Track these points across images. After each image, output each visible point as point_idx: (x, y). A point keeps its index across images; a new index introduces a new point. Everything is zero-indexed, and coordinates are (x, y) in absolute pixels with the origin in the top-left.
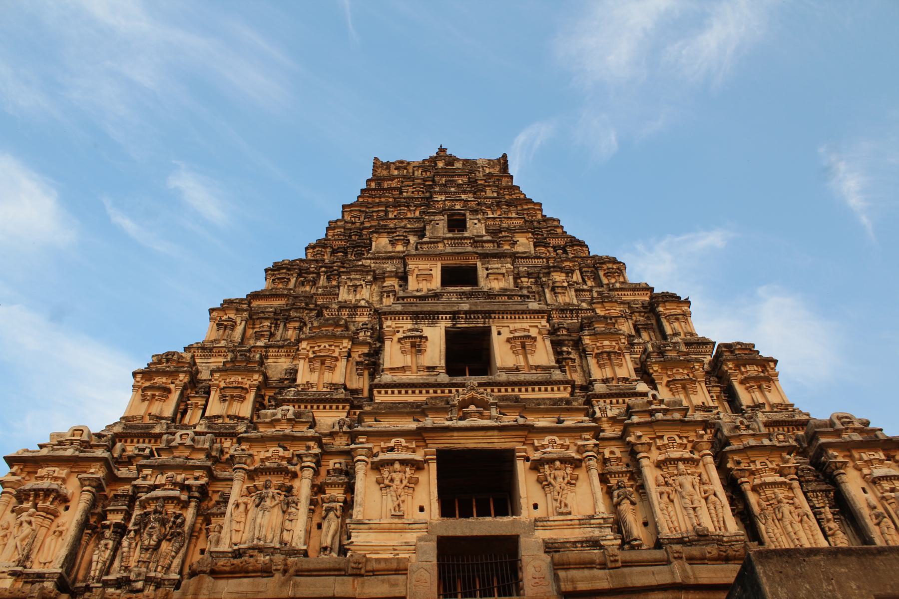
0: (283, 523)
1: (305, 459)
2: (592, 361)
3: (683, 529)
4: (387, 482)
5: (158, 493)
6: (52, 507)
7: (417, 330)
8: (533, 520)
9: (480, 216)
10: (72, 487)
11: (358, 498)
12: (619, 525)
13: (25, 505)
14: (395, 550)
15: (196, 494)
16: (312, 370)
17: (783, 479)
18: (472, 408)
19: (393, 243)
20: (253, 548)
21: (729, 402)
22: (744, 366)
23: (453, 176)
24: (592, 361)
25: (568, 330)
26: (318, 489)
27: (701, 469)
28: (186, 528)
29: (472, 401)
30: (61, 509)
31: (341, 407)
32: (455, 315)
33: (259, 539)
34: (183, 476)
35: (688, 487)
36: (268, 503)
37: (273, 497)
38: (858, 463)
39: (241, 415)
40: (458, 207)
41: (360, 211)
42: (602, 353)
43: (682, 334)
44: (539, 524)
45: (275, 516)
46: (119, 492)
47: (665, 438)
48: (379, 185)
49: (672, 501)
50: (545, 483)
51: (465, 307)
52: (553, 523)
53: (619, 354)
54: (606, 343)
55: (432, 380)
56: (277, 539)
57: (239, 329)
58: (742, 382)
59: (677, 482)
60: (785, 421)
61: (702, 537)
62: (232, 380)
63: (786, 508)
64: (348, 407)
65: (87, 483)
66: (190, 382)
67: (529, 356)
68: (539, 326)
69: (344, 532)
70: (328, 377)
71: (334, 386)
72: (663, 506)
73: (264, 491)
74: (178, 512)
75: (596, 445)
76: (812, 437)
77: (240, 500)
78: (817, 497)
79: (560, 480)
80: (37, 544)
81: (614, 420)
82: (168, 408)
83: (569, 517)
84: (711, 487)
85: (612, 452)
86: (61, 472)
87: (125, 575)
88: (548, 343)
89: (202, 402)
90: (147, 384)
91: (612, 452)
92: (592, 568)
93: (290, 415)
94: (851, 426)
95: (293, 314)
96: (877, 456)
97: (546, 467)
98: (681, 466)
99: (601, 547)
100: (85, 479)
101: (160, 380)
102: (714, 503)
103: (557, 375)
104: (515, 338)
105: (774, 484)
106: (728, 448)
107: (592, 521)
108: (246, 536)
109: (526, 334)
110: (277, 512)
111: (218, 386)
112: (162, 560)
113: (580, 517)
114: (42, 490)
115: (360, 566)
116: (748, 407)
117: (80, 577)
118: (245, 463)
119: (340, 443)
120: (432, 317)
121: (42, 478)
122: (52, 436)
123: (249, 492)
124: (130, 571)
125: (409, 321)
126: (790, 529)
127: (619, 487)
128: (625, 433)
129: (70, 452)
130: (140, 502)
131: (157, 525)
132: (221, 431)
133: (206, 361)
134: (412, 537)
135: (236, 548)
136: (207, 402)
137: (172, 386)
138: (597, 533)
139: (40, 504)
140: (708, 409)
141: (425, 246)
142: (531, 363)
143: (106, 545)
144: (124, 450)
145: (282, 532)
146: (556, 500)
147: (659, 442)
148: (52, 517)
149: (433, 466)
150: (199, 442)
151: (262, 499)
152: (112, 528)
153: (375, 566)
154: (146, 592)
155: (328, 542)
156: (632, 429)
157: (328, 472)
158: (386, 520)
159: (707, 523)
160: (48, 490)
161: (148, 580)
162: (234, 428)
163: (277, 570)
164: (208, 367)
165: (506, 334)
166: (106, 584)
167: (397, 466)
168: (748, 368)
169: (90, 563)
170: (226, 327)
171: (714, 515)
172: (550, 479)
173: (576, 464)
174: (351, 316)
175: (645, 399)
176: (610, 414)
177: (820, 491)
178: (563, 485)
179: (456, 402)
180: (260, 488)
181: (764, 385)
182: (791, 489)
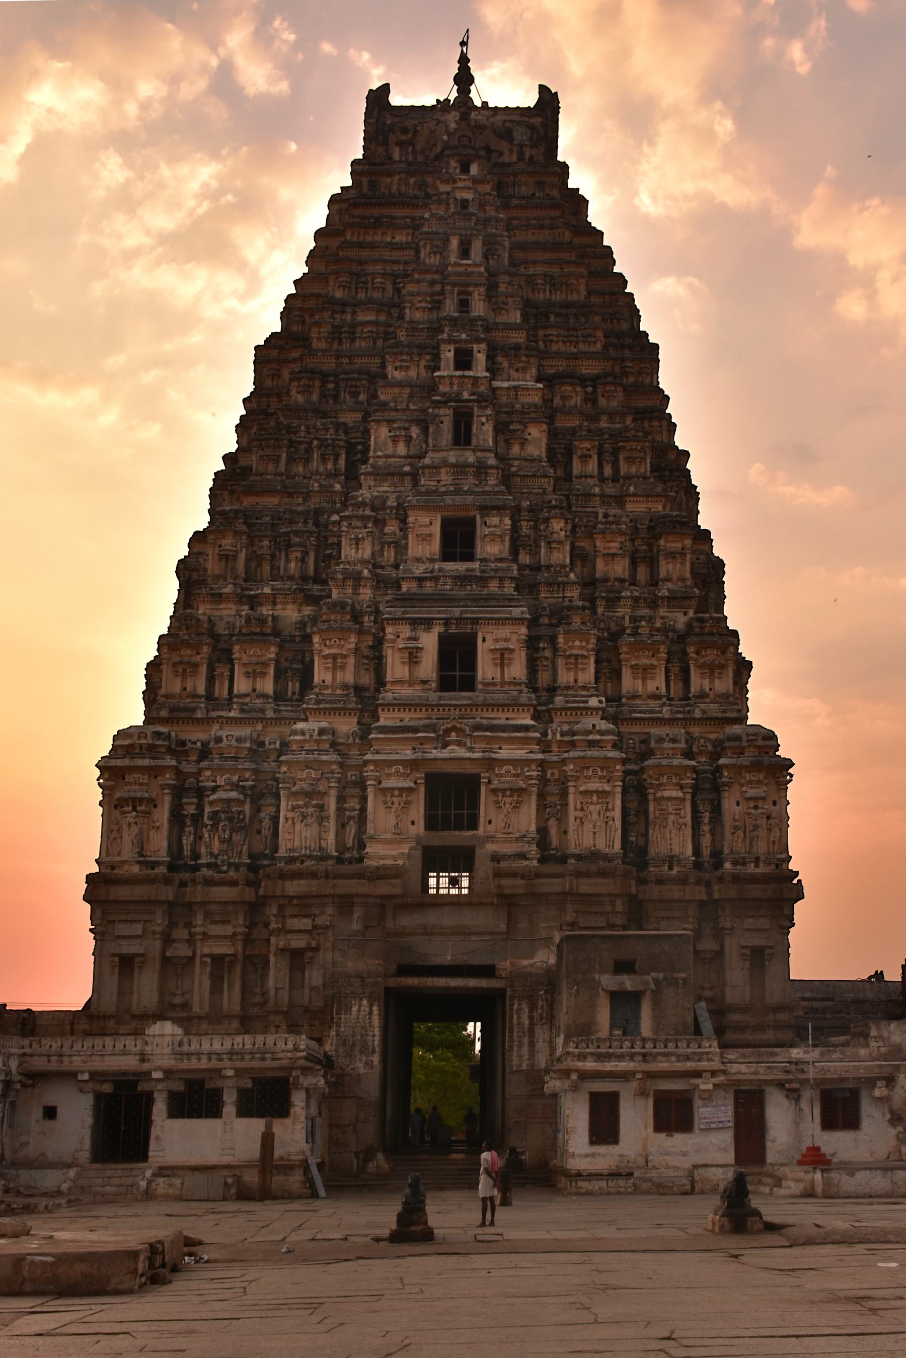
0: (320, 834)
4: (389, 804)
5: (221, 794)
7: (415, 639)
9: (489, 411)
11: (370, 816)
19: (395, 440)
20: (305, 856)
23: (468, 286)
25: (550, 617)
26: (341, 799)
28: (247, 821)
32: (447, 622)
36: (309, 820)
40: (466, 395)
41: (351, 273)
45: (315, 828)
48: (373, 185)
51: (456, 612)
54: (577, 643)
56: (317, 846)
57: (242, 556)
67: (506, 669)
71: (345, 686)
79: (508, 806)
86: (145, 779)
101: (186, 652)
104: (496, 650)
110: (315, 825)
111: (240, 659)
120: (428, 623)
123: (293, 808)
125: (408, 627)
128: (564, 762)
129: (146, 762)
131: (227, 823)
134: (405, 849)
139: (138, 808)
141: (427, 471)
143: (190, 832)
149: (422, 789)
151: (304, 817)
158: (388, 836)
161: (230, 865)
164: (221, 618)
165: (490, 645)
167: (396, 793)
170: (227, 556)
172: (502, 804)
174: (356, 587)
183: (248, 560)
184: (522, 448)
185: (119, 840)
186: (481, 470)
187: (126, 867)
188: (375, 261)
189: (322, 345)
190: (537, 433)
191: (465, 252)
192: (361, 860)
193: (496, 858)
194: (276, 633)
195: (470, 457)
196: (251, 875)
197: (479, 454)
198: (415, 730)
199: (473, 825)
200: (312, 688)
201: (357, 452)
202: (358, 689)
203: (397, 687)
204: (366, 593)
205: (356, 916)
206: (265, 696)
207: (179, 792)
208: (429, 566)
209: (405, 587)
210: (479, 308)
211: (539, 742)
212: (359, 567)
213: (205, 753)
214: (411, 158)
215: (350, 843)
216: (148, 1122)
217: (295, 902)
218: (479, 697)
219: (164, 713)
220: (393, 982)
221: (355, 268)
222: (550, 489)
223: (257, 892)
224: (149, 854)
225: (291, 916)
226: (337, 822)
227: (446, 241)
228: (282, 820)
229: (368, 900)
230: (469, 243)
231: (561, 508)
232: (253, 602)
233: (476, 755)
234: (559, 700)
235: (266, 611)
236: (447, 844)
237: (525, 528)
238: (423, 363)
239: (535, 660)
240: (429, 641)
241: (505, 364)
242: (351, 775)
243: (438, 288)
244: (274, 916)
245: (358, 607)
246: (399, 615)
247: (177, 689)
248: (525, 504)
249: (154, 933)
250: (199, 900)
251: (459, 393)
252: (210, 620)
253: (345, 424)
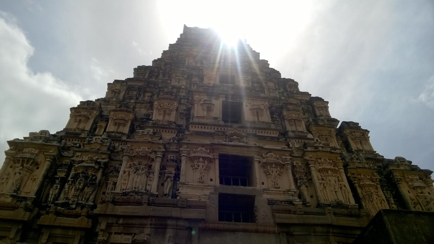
0: (146, 182)
1: (158, 153)
2: (287, 123)
3: (330, 200)
4: (196, 166)
6: (31, 167)
7: (210, 101)
8: (262, 189)
10: (40, 159)
12: (300, 196)
13: (17, 165)
14: (199, 197)
15: (103, 166)
16: (160, 114)
17: (373, 183)
18: (235, 137)
20: (133, 192)
21: (346, 148)
22: (354, 132)
24: (287, 123)
26: (163, 168)
28: (97, 182)
29: (235, 134)
31: (173, 132)
33: (135, 188)
34: (97, 157)
36: (140, 172)
37: (143, 169)
38: (407, 180)
39: (124, 132)
42: (292, 119)
43: (324, 116)
44: (265, 191)
46: (64, 163)
47: (322, 159)
49: (325, 187)
50: (267, 173)
52: (271, 192)
53: (299, 121)
54: (294, 115)
55: (216, 123)
56: (144, 188)
57: (122, 94)
58: (352, 139)
59: (328, 179)
60: (372, 158)
61: (339, 205)
62: (120, 116)
63: (375, 197)
64: (176, 132)
65: (48, 157)
66: (98, 116)
67: (260, 118)
68: (264, 104)
69: (175, 187)
70: (167, 118)
71: (170, 123)
72: (321, 189)
73: (138, 166)
74: (94, 174)
75: (291, 159)
76: (387, 166)
77: (126, 170)
78: (388, 193)
79: (274, 172)
81: (298, 149)
82: (88, 127)
83: (279, 190)
84: (343, 183)
85: (297, 163)
87: (67, 201)
88: (268, 112)
89: (104, 125)
90: (78, 114)
91: (297, 163)
92: (290, 213)
93: (151, 133)
94: (404, 163)
95: (147, 89)
96: (415, 177)
97: (269, 166)
98: (330, 172)
99: (294, 205)
100: (47, 155)
102: (345, 190)
103: (273, 126)
104: (254, 109)
105: (370, 185)
106: (348, 167)
107: (289, 192)
108: (129, 186)
109: (259, 107)
112: (85, 195)
113: (284, 190)
114: (26, 158)
115: (184, 203)
116: (355, 150)
117: (43, 200)
118: (129, 153)
119: (173, 148)
121: (26, 153)
122: (31, 134)
123: (130, 167)
124: (69, 200)
126: (376, 206)
127: (300, 179)
129: (40, 142)
130: (75, 168)
131: (83, 179)
132: (115, 138)
133: (106, 107)
134: (207, 192)
135: (124, 191)
136: (107, 125)
137: (90, 116)
138: (291, 198)
139: (25, 165)
142: (261, 120)
144: (65, 144)
145: (146, 186)
146: (273, 181)
147: (319, 161)
148: (31, 172)
149: (217, 162)
150: (104, 143)
151: (137, 170)
152: (59, 179)
154: (77, 210)
155: (167, 191)
156: (307, 153)
157: (167, 160)
159: (341, 198)
160: (29, 158)
161: (78, 204)
162: (120, 137)
163: (144, 202)
166: (57, 205)
167: (201, 160)
168: (356, 133)
169: (48, 194)
170: (115, 93)
171: (344, 196)
173: (282, 166)
175: (313, 142)
176: (296, 146)
177: (389, 190)
178: (276, 175)
179: (228, 134)
180: (136, 165)
181: (363, 142)
182: (377, 188)
185: (5, 184)
205: (168, 236)
217: (121, 221)
225: (116, 233)
226: (159, 181)
229: (179, 223)
236: (236, 193)
242: (170, 156)
244: (102, 230)
250: (47, 224)
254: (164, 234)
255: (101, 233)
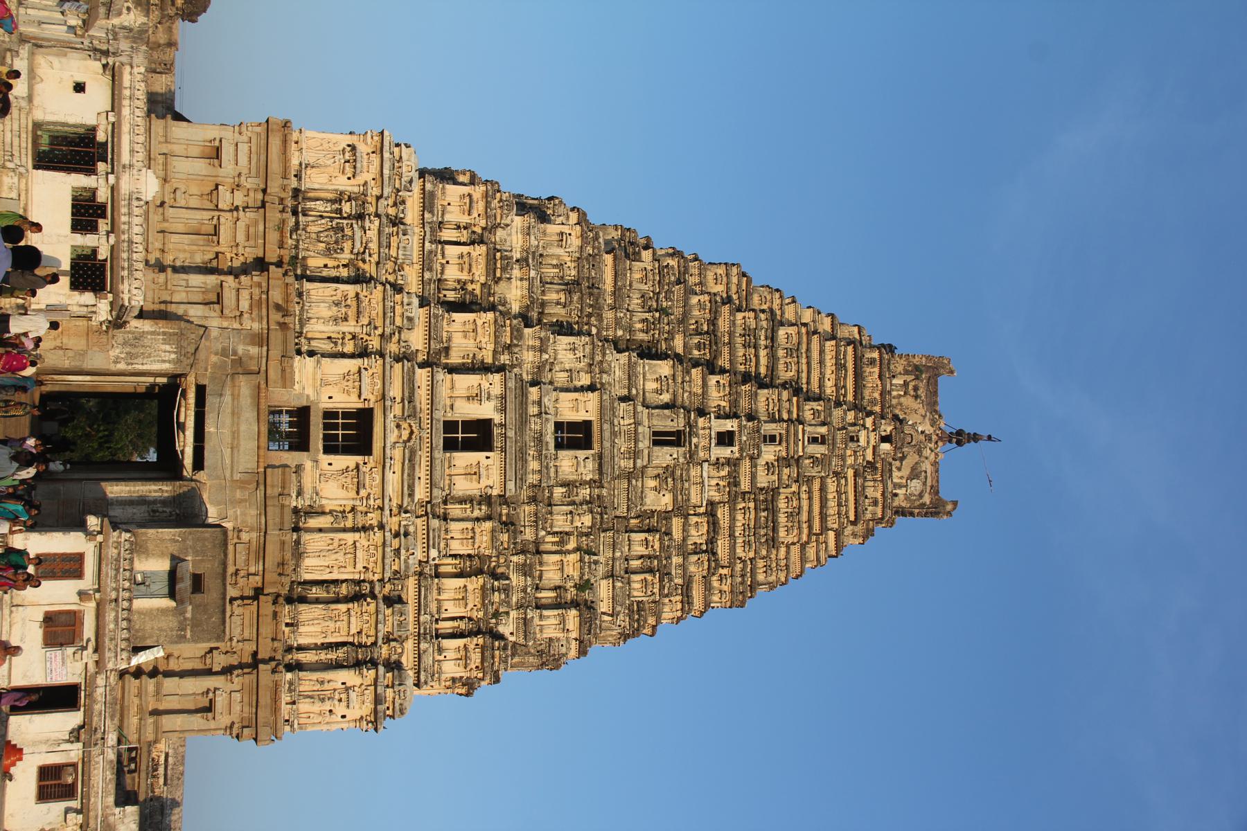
5: (358, 233)
9: (682, 460)
12: (313, 512)
17: (353, 631)
24: (469, 525)
25: (508, 515)
27: (350, 569)
29: (412, 433)
30: (350, 175)
35: (334, 557)
40: (694, 440)
48: (872, 362)
51: (511, 434)
54: (485, 538)
63: (331, 624)
71: (449, 339)
80: (322, 169)
101: (480, 207)
110: (330, 314)
120: (503, 410)
129: (386, 172)
134: (309, 391)
138: (307, 496)
140: (439, 612)
149: (360, 406)
151: (337, 305)
153: (288, 370)
161: (298, 241)
164: (510, 235)
165: (484, 462)
174: (533, 347)
183: (558, 257)
184: (651, 489)
186: (635, 454)
187: (297, 153)
188: (808, 364)
189: (739, 322)
190: (665, 501)
191: (814, 440)
192: (299, 352)
193: (299, 469)
194: (497, 281)
195: (641, 445)
196: (286, 259)
197: (646, 452)
198: (411, 399)
199: (328, 450)
200: (448, 312)
201: (649, 352)
202: (447, 349)
203: (448, 384)
204: (529, 357)
205: (250, 348)
206: (442, 273)
207: (359, 199)
208: (552, 411)
209: (534, 392)
210: (769, 453)
211: (400, 507)
212: (550, 351)
213: (396, 222)
214: (894, 393)
215: (313, 343)
216: (68, 170)
218: (439, 454)
219: (429, 186)
220: (191, 380)
221: (804, 347)
222: (618, 513)
223: (272, 264)
224: (309, 172)
227: (823, 424)
228: (334, 285)
230: (823, 443)
231: (601, 523)
232: (523, 261)
233: (388, 451)
234: (435, 523)
235: (516, 272)
237: (585, 492)
238: (723, 404)
239: (471, 501)
240: (487, 410)
241: (723, 473)
242: (375, 343)
243: (785, 416)
245: (516, 350)
246: (509, 385)
247: (448, 199)
248: (604, 492)
249: (240, 175)
251: (697, 435)
252: (507, 225)
253: (673, 339)
254: (253, 344)
255: (249, 277)
